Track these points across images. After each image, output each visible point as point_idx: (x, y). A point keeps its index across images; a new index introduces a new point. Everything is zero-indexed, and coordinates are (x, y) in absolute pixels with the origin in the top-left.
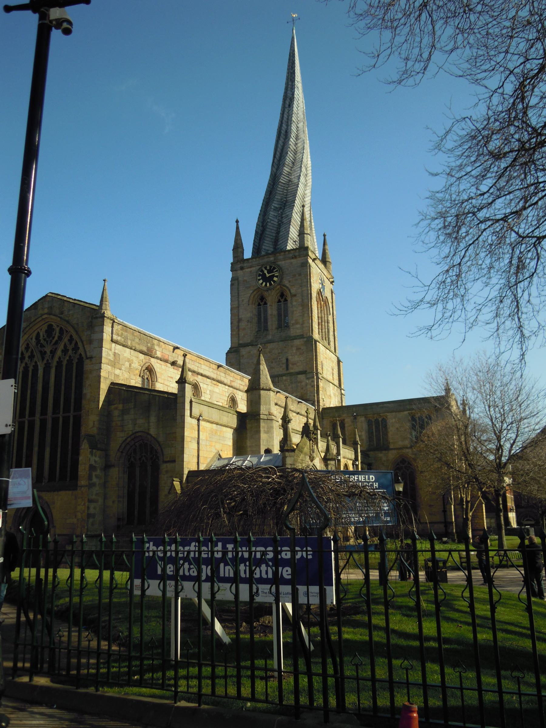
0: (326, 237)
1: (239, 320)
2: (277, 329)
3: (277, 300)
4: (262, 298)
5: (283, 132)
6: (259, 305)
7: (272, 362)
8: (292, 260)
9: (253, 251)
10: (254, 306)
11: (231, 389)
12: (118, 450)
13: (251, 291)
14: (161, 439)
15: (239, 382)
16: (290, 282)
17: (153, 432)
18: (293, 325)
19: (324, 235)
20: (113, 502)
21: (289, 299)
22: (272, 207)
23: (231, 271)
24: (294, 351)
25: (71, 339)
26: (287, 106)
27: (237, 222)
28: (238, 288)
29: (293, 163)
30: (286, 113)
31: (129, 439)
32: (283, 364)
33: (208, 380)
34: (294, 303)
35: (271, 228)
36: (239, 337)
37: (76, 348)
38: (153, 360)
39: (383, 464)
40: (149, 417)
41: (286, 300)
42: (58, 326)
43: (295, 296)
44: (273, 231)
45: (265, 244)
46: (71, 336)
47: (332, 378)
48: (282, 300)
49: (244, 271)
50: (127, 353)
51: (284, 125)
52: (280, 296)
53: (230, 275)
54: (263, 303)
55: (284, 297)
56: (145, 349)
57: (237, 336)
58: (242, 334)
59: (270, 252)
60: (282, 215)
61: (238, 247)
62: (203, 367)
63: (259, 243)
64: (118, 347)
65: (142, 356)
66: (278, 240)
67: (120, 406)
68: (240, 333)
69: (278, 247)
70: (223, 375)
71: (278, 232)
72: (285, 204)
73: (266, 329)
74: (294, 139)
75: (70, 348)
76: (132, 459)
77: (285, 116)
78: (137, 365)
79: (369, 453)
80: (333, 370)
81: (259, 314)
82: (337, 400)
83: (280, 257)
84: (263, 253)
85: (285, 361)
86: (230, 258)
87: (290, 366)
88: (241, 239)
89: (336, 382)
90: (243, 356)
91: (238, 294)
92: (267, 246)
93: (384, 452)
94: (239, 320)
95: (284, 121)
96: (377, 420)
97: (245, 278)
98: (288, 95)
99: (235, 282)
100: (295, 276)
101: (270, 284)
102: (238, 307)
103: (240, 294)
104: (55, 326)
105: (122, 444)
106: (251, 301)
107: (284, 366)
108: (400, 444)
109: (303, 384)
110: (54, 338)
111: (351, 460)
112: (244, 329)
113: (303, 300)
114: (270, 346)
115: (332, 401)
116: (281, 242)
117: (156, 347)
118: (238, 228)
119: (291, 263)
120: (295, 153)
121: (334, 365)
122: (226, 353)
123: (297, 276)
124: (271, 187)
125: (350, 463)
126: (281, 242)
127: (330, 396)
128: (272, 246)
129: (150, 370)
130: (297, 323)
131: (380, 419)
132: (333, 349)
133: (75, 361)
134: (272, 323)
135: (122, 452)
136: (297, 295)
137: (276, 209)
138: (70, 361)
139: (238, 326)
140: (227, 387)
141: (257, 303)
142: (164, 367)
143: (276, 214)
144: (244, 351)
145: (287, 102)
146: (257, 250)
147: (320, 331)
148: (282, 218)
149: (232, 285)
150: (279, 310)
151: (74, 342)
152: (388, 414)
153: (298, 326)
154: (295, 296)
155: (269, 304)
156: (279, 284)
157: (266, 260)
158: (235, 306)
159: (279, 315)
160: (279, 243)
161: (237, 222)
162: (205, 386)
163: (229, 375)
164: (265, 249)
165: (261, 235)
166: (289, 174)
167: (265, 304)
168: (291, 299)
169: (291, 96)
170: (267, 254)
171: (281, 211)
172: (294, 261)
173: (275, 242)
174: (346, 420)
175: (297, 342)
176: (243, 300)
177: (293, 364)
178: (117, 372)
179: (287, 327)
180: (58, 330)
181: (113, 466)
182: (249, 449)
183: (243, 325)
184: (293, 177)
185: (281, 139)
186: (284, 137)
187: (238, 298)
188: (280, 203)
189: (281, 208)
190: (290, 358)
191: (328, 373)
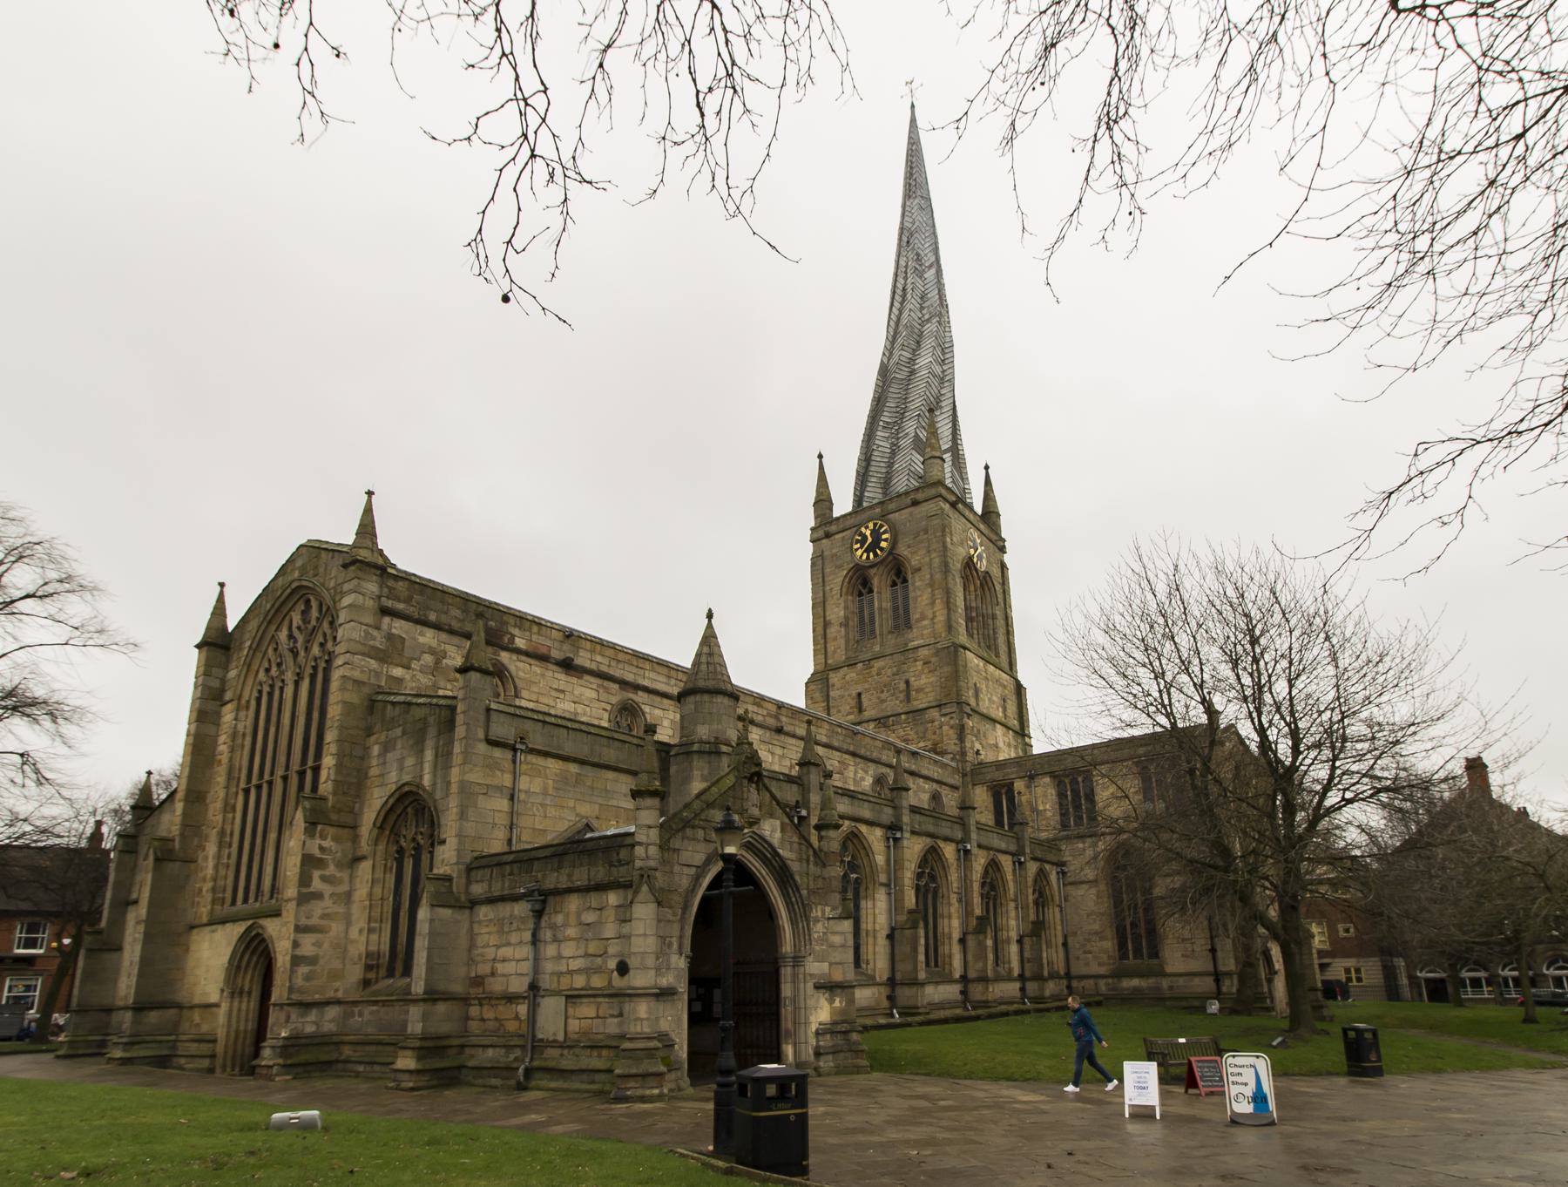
1: (826, 624)
6: (861, 594)
18: (918, 621)
33: (666, 701)
41: (905, 581)
53: (809, 549)
58: (831, 648)
61: (823, 501)
62: (653, 675)
81: (861, 611)
83: (892, 506)
85: (902, 686)
94: (826, 624)
99: (819, 564)
101: (876, 555)
107: (902, 696)
114: (878, 664)
130: (923, 618)
132: (1005, 665)
134: (883, 622)
144: (835, 678)
149: (813, 565)
150: (894, 599)
153: (925, 622)
156: (890, 553)
159: (895, 609)
162: (657, 712)
167: (871, 591)
177: (919, 690)
183: (832, 631)
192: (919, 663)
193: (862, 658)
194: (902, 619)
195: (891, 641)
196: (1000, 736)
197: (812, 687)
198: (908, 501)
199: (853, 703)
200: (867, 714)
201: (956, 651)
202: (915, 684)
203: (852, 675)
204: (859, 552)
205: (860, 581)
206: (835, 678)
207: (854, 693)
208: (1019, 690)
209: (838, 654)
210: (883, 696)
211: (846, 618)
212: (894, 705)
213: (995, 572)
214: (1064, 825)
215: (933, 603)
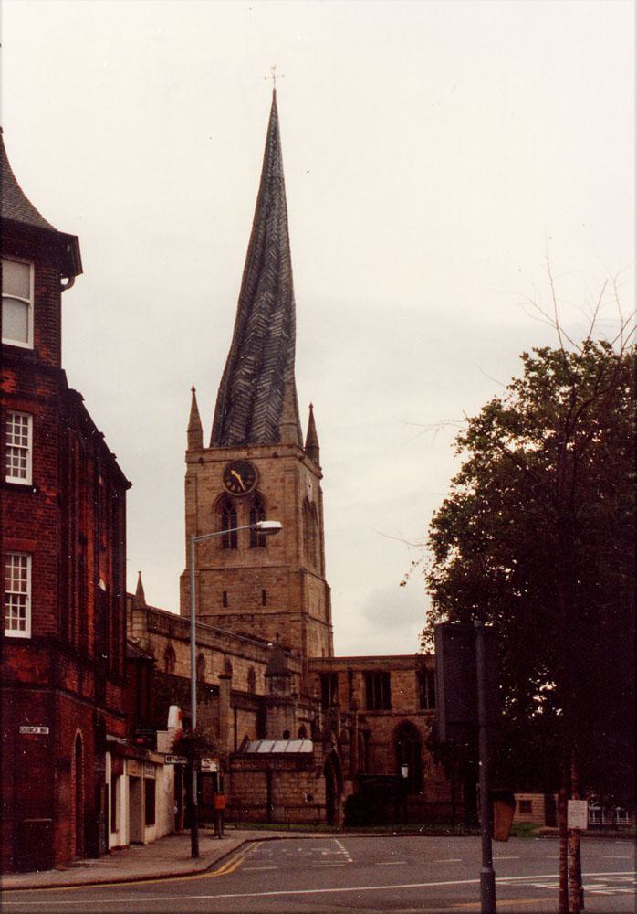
0: (313, 409)
2: (251, 547)
9: (213, 430)
19: (311, 407)
22: (243, 373)
26: (263, 216)
27: (194, 390)
38: (173, 642)
53: (184, 468)
59: (240, 440)
61: (195, 430)
65: (165, 640)
69: (251, 434)
83: (256, 453)
85: (260, 592)
86: (185, 446)
88: (198, 418)
89: (322, 618)
92: (236, 432)
99: (190, 480)
107: (261, 600)
108: (407, 708)
116: (255, 428)
126: (255, 428)
137: (248, 377)
142: (179, 645)
143: (248, 384)
149: (188, 482)
161: (194, 390)
172: (275, 461)
190: (267, 589)
199: (221, 598)
201: (302, 576)
207: (220, 591)
208: (327, 589)
213: (317, 504)
214: (369, 705)
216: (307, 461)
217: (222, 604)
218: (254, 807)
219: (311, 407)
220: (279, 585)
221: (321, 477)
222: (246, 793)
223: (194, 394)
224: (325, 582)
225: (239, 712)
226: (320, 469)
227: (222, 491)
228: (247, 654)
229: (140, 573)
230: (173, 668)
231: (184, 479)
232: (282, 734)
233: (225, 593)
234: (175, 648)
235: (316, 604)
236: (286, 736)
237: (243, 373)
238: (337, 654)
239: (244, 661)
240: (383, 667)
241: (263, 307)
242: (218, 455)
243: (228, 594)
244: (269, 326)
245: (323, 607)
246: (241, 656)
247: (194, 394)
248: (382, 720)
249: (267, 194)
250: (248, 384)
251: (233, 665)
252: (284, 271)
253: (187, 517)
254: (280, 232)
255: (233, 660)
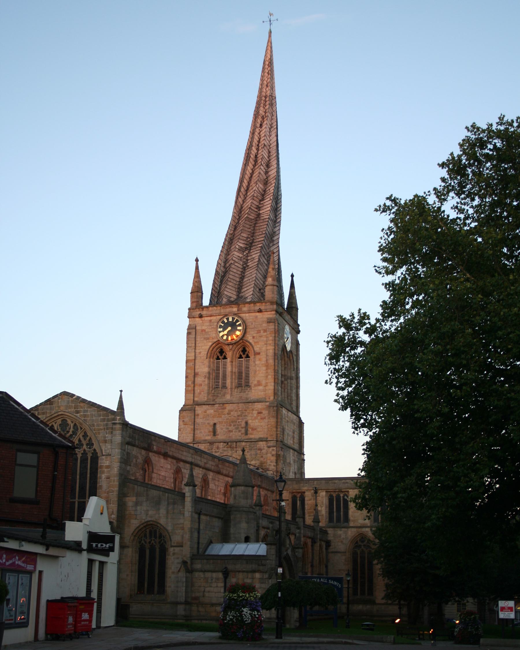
0: (294, 278)
1: (195, 375)
3: (238, 356)
4: (222, 352)
5: (252, 156)
6: (218, 358)
7: (230, 425)
8: (258, 314)
10: (212, 360)
11: (204, 470)
12: (132, 534)
13: (210, 344)
14: (169, 528)
15: (211, 463)
16: (253, 337)
17: (162, 521)
19: (292, 276)
20: (127, 575)
21: (252, 357)
22: (237, 247)
23: (189, 317)
24: (255, 415)
25: (85, 435)
26: (258, 125)
27: (197, 260)
28: (195, 338)
29: (263, 195)
30: (256, 133)
31: (142, 526)
32: (242, 428)
34: (257, 362)
35: (235, 271)
36: (194, 393)
37: (90, 444)
38: (150, 454)
39: (342, 542)
40: (159, 509)
41: (248, 356)
42: (72, 422)
43: (259, 354)
44: (237, 275)
45: (227, 289)
46: (85, 433)
47: (292, 442)
48: (243, 356)
49: (203, 319)
50: (135, 451)
51: (254, 149)
52: (242, 351)
53: (186, 322)
54: (223, 357)
55: (246, 353)
56: (146, 446)
57: (193, 392)
59: (232, 299)
60: (247, 257)
61: (197, 291)
62: (185, 453)
63: (220, 286)
64: (130, 447)
65: (143, 452)
66: (242, 286)
67: (134, 499)
68: (196, 388)
69: (242, 294)
70: (199, 458)
71: (242, 278)
72: (251, 243)
73: (224, 386)
74: (265, 167)
75: (84, 442)
76: (143, 542)
77: (256, 138)
78: (140, 460)
79: (328, 529)
80: (294, 433)
82: (296, 467)
83: (245, 309)
84: (225, 300)
85: (243, 424)
86: (187, 303)
87: (250, 430)
89: (296, 447)
90: (198, 415)
91: (195, 344)
92: (229, 292)
93: (343, 529)
95: (254, 144)
96: (338, 497)
97: (204, 328)
98: (261, 112)
99: (191, 330)
100: (259, 332)
102: (195, 360)
103: (197, 345)
104: (69, 422)
105: (135, 530)
106: (209, 354)
107: (243, 430)
109: (263, 451)
110: (68, 432)
111: (310, 538)
112: (201, 385)
113: (267, 360)
114: (229, 407)
115: (292, 468)
116: (246, 289)
117: (154, 443)
118: (197, 268)
119: (256, 317)
120: (266, 183)
121: (295, 427)
122: (180, 411)
123: (262, 332)
124: (236, 221)
125: (309, 541)
126: (246, 289)
127: (290, 463)
128: (235, 293)
129: (147, 461)
130: (259, 384)
131: (342, 495)
132: (294, 409)
133: (89, 456)
135: (135, 536)
136: (261, 354)
137: (241, 250)
138: (85, 453)
139: (194, 382)
140: (201, 469)
141: (215, 357)
142: (157, 458)
143: (241, 255)
144: (199, 410)
145: (259, 121)
146: (217, 294)
147: (283, 390)
148: (247, 260)
149: (189, 334)
150: (240, 366)
151: (88, 438)
152: (350, 490)
153: (261, 388)
154: (259, 354)
155: (229, 360)
157: (228, 310)
158: (190, 358)
160: (243, 290)
161: (197, 260)
163: (204, 458)
164: (227, 295)
165: (223, 277)
166: (259, 208)
167: (225, 358)
168: (254, 358)
169: (263, 114)
170: (230, 303)
171: (247, 252)
173: (238, 288)
174: (306, 493)
175: (259, 406)
176: (200, 353)
177: (253, 429)
178: (128, 468)
179: (248, 385)
180: (72, 425)
181: (128, 547)
182: (232, 536)
183: (199, 380)
184: (261, 212)
185: (250, 164)
186: (253, 163)
187: (195, 349)
188: (246, 242)
189: (246, 248)
191: (289, 438)
192: (255, 412)
193: (218, 400)
194: (243, 381)
195: (237, 394)
196: (291, 456)
197: (184, 413)
198: (257, 308)
199: (211, 429)
200: (221, 437)
202: (253, 423)
203: (211, 411)
204: (221, 334)
205: (219, 352)
206: (199, 410)
207: (212, 423)
208: (301, 424)
209: (202, 396)
210: (230, 428)
211: (209, 373)
212: (236, 435)
214: (331, 519)
215: (267, 377)
216: (288, 317)
217: (212, 434)
218: (213, 605)
219: (292, 276)
220: (259, 418)
221: (298, 332)
222: (204, 591)
223: (197, 264)
224: (300, 418)
225: (203, 517)
226: (299, 325)
227: (215, 340)
228: (225, 472)
229: (121, 391)
230: (151, 478)
231: (186, 332)
232: (243, 539)
233: (215, 424)
234: (154, 462)
235: (291, 433)
236: (247, 540)
237: (237, 247)
238: (308, 475)
239: (221, 477)
240: (342, 486)
241: (255, 195)
242: (215, 310)
243: (218, 426)
244: (259, 210)
245: (296, 437)
246: (219, 473)
247: (197, 264)
248: (340, 532)
249: (262, 108)
250: (241, 255)
251: (210, 480)
252: (272, 168)
253: (187, 361)
254: (271, 138)
255: (211, 475)
